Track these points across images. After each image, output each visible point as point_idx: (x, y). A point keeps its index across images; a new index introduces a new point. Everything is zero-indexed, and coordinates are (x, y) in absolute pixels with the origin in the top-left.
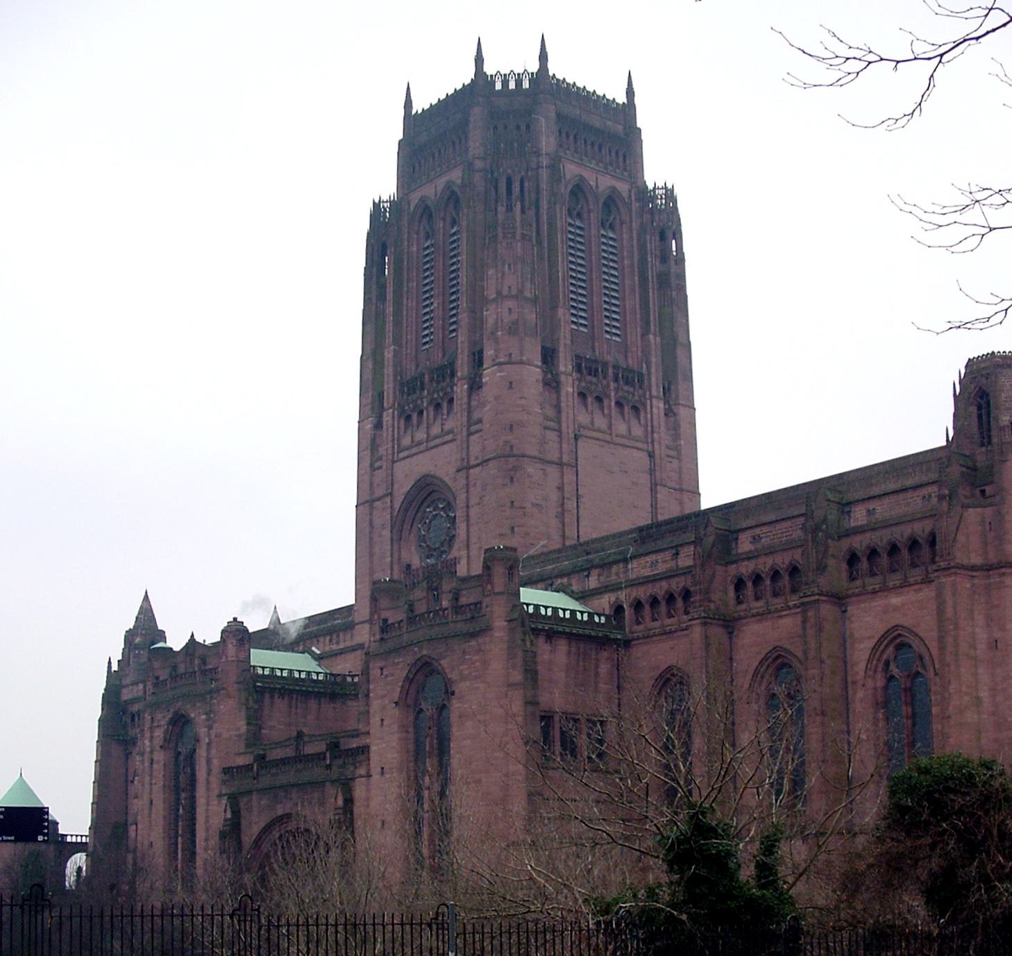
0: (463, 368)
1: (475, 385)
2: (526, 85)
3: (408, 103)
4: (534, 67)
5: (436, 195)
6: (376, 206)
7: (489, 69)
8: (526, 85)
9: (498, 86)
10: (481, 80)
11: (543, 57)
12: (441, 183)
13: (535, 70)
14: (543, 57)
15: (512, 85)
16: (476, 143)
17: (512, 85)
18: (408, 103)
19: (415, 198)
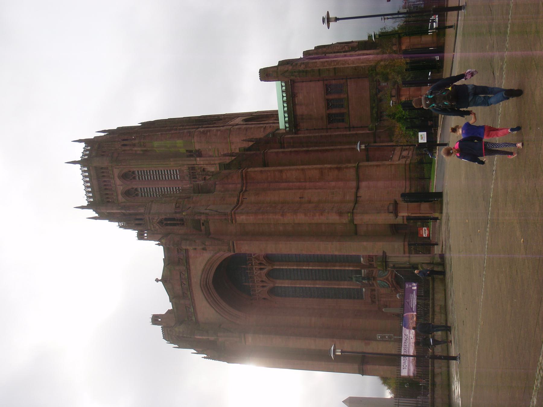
0: (191, 162)
1: (199, 154)
2: (89, 148)
3: (83, 207)
4: (83, 145)
5: (122, 185)
6: (121, 227)
7: (80, 159)
8: (89, 148)
9: (86, 157)
10: (82, 162)
11: (80, 141)
12: (118, 182)
13: (85, 145)
14: (80, 141)
15: (88, 152)
16: (105, 162)
17: (88, 152)
18: (83, 207)
19: (121, 198)
